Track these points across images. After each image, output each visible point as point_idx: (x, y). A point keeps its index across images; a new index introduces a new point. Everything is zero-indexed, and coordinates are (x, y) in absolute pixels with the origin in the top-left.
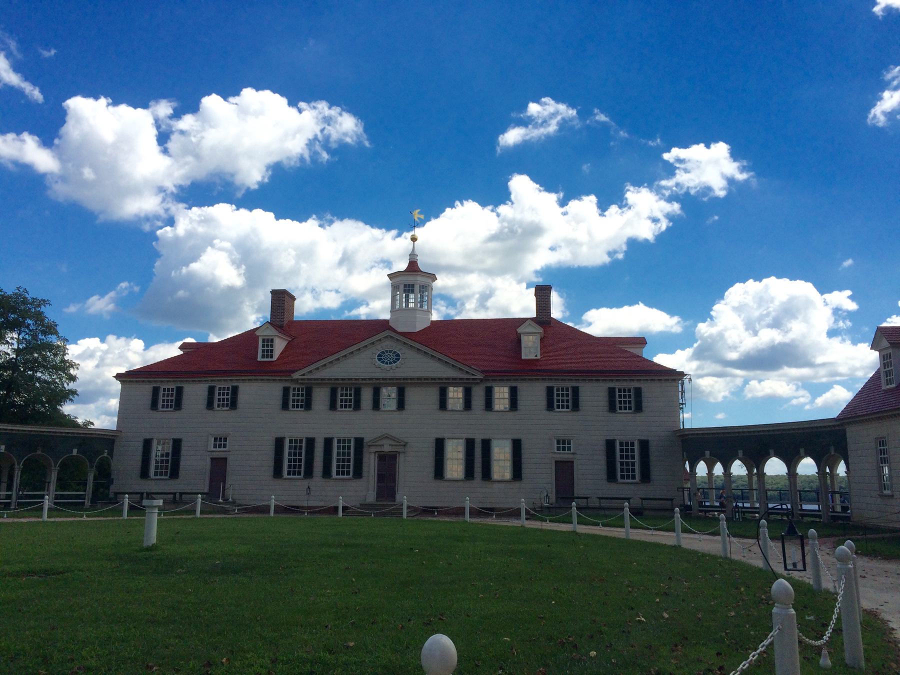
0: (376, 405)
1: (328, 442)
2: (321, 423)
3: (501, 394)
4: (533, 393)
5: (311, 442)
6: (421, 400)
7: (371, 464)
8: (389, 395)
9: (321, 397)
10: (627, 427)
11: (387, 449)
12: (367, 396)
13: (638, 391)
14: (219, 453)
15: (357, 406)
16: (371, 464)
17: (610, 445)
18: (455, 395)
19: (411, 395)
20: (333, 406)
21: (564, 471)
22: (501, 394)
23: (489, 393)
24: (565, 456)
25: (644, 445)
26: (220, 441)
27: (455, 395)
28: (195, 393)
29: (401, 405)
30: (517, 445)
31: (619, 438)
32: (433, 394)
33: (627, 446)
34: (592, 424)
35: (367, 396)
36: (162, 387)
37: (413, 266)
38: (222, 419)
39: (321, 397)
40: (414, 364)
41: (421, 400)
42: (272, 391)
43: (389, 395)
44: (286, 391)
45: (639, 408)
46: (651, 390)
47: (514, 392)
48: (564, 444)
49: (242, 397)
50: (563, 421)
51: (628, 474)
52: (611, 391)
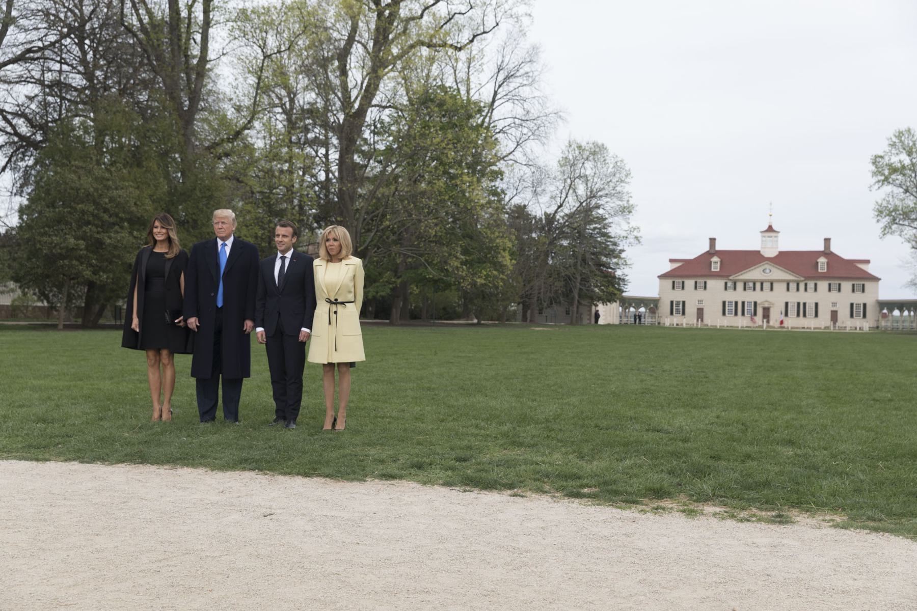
0: (762, 289)
1: (743, 303)
2: (739, 295)
3: (811, 285)
4: (823, 285)
5: (736, 303)
6: (780, 288)
7: (760, 311)
8: (767, 286)
9: (740, 286)
10: (858, 298)
11: (766, 305)
12: (758, 286)
13: (863, 285)
14: (700, 306)
15: (754, 289)
16: (760, 311)
17: (852, 305)
18: (793, 286)
19: (775, 285)
20: (745, 289)
21: (834, 315)
22: (811, 285)
23: (806, 285)
24: (834, 309)
25: (865, 305)
26: (700, 302)
27: (793, 286)
28: (689, 283)
29: (772, 289)
30: (817, 304)
31: (855, 302)
32: (785, 285)
33: (858, 305)
34: (846, 296)
35: (758, 286)
36: (676, 281)
37: (770, 229)
38: (700, 293)
39: (740, 286)
40: (777, 274)
41: (780, 288)
42: (720, 283)
43: (767, 286)
44: (726, 283)
45: (863, 291)
46: (869, 285)
47: (816, 285)
48: (834, 304)
49: (708, 286)
50: (834, 295)
51: (858, 315)
52: (853, 285)
